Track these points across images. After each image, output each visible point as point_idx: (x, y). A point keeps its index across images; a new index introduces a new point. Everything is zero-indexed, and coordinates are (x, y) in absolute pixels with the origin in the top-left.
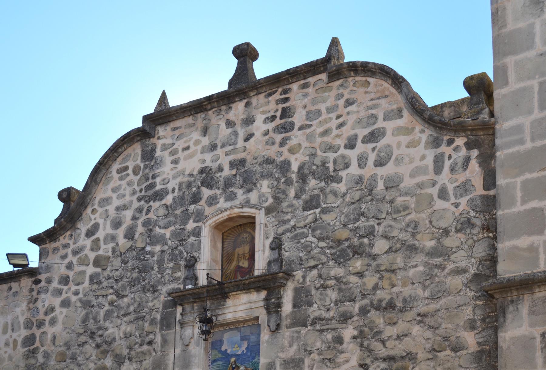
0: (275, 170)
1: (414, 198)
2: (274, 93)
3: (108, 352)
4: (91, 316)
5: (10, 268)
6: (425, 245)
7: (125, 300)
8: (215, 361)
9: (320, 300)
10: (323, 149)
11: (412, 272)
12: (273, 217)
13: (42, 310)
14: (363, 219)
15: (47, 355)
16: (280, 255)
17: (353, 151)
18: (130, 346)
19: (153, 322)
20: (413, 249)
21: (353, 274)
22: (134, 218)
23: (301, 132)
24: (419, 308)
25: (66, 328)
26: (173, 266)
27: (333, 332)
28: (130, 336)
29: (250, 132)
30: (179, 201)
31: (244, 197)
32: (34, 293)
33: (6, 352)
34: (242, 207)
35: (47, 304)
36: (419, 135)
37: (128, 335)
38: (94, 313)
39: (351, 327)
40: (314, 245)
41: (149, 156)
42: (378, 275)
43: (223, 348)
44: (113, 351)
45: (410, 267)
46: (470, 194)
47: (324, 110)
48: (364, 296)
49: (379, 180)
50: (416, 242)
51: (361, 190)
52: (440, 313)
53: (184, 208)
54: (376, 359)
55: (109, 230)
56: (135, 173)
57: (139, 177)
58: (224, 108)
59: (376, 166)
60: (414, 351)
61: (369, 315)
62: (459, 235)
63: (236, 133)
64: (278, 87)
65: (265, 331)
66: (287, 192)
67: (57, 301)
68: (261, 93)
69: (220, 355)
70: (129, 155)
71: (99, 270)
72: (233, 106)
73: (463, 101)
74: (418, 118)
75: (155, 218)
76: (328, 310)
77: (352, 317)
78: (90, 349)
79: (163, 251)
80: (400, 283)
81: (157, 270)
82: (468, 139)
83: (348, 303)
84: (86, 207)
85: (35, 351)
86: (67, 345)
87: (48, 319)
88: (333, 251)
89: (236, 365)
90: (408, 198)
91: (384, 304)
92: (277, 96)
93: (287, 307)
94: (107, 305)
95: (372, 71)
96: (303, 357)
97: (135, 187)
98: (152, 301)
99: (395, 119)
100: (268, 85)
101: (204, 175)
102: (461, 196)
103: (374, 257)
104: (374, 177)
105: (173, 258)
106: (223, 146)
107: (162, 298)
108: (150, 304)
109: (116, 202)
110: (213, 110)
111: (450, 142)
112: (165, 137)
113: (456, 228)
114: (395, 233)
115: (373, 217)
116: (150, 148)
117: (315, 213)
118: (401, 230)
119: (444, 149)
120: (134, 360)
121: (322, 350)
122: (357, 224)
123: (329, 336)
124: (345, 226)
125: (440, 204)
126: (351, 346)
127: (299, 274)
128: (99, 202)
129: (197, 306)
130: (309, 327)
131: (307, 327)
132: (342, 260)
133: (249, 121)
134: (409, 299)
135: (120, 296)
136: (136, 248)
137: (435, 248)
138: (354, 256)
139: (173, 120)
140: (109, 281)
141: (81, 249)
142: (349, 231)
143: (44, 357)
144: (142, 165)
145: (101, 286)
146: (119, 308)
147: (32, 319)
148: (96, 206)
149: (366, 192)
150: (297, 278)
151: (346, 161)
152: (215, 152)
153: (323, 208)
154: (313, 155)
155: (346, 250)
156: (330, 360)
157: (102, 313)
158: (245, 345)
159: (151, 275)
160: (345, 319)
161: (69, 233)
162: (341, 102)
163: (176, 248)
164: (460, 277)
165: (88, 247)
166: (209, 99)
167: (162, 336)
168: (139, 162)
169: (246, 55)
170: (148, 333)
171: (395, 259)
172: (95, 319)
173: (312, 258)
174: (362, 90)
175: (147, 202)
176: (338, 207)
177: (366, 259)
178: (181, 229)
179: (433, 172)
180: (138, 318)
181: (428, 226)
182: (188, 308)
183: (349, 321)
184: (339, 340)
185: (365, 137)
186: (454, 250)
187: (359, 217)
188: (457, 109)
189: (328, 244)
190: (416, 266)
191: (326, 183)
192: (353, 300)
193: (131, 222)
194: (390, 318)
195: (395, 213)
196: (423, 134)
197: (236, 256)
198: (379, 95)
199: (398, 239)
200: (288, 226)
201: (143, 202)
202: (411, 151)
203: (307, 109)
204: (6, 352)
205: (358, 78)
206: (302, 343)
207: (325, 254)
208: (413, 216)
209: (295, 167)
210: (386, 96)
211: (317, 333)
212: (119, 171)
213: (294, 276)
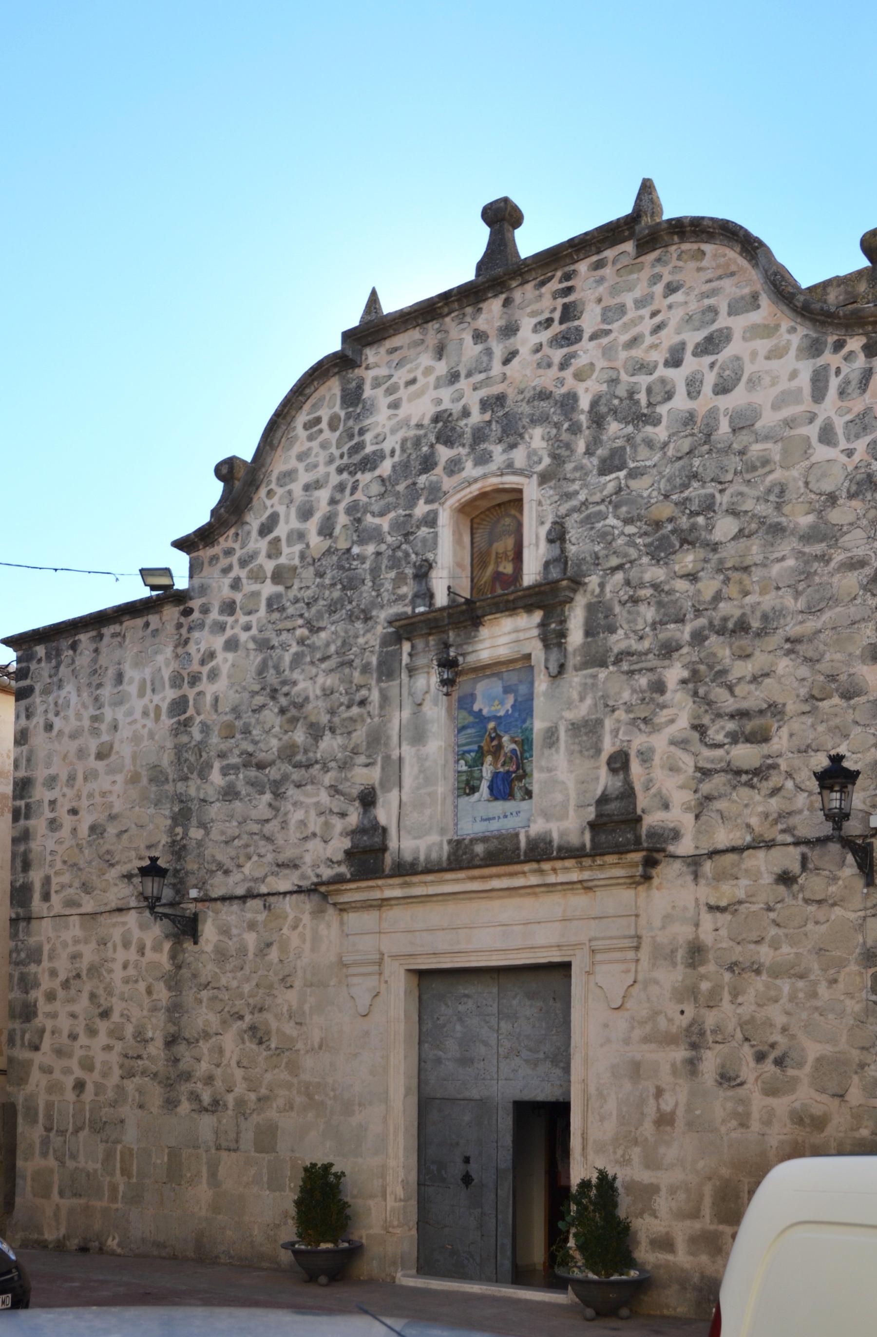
0: (552, 410)
1: (780, 444)
2: (550, 279)
3: (298, 720)
4: (270, 663)
5: (145, 592)
6: (797, 523)
7: (323, 635)
8: (464, 728)
9: (629, 622)
10: (631, 370)
11: (776, 569)
12: (551, 488)
13: (196, 658)
14: (695, 484)
15: (206, 729)
16: (563, 550)
17: (678, 369)
19: (366, 669)
20: (777, 530)
21: (681, 577)
22: (333, 502)
23: (593, 343)
24: (787, 628)
25: (233, 684)
27: (649, 674)
28: (332, 693)
29: (512, 349)
30: (403, 469)
31: (505, 457)
32: (184, 631)
33: (144, 726)
34: (502, 475)
35: (203, 647)
36: (787, 336)
37: (328, 692)
38: (275, 659)
39: (678, 665)
40: (616, 532)
41: (353, 398)
42: (722, 577)
43: (476, 708)
44: (305, 718)
45: (772, 561)
46: (871, 433)
47: (630, 304)
48: (698, 613)
49: (722, 418)
50: (783, 519)
51: (693, 435)
52: (822, 636)
53: (409, 481)
54: (719, 715)
55: (295, 524)
56: (333, 427)
57: (337, 433)
58: (469, 310)
59: (716, 393)
60: (780, 701)
61: (707, 643)
62: (855, 503)
63: (489, 352)
64: (556, 270)
65: (542, 677)
66: (573, 446)
67: (218, 643)
68: (528, 282)
69: (471, 719)
70: (322, 399)
71: (280, 589)
72: (484, 306)
73: (860, 274)
74: (785, 308)
75: (365, 499)
76: (641, 638)
77: (679, 648)
78: (270, 716)
79: (378, 554)
80: (757, 588)
81: (370, 584)
82: (869, 338)
83: (673, 626)
84: (258, 488)
85: (187, 723)
86: (236, 711)
87: (205, 670)
88: (648, 540)
90: (769, 445)
91: (730, 625)
92: (555, 285)
93: (576, 637)
94: (294, 644)
95: (708, 232)
97: (333, 450)
98: (364, 635)
99: (747, 311)
100: (539, 267)
101: (440, 425)
102: (857, 437)
103: (715, 547)
104: (713, 414)
105: (395, 563)
106: (469, 375)
107: (380, 630)
109: (304, 477)
110: (453, 315)
111: (839, 346)
112: (377, 365)
113: (848, 491)
114: (748, 505)
115: (712, 480)
116: (354, 384)
117: (618, 478)
118: (758, 499)
119: (830, 358)
120: (338, 731)
122: (686, 494)
123: (643, 681)
124: (666, 497)
125: (822, 452)
126: (679, 696)
127: (593, 581)
128: (278, 479)
130: (611, 668)
132: (662, 555)
133: (510, 330)
134: (771, 615)
135: (315, 630)
136: (337, 550)
137: (813, 527)
138: (681, 546)
139: (390, 337)
140: (297, 605)
141: (252, 556)
142: (672, 505)
143: (202, 732)
144: (342, 414)
145: (285, 615)
146: (313, 648)
147: (182, 672)
148: (273, 486)
149: (700, 439)
150: (590, 587)
151: (668, 388)
152: (457, 386)
154: (614, 382)
155: (668, 537)
156: (645, 720)
157: (287, 658)
158: (510, 700)
159: (361, 593)
161: (232, 531)
162: (659, 289)
163: (399, 547)
164: (856, 573)
165: (263, 553)
166: (446, 297)
167: (381, 691)
168: (337, 409)
169: (503, 219)
170: (359, 687)
171: (748, 548)
172: (276, 667)
173: (615, 553)
174: (692, 265)
175: (352, 474)
176: (654, 466)
177: (701, 550)
178: (406, 515)
179: (810, 399)
180: (342, 664)
181: (802, 490)
182: (420, 643)
183: (675, 655)
184: (659, 687)
185: (697, 345)
186: (845, 529)
187: (690, 480)
188: (850, 289)
189: (640, 528)
190: (783, 559)
191: (636, 426)
192: (681, 620)
193: (328, 509)
194: (741, 648)
195: (747, 471)
196: (793, 334)
197: (493, 556)
198: (720, 272)
199: (754, 516)
200: (575, 503)
201: (345, 475)
202: (774, 364)
203: (603, 304)
204: (144, 726)
205: (686, 246)
206: (600, 694)
207: (635, 545)
208: (777, 475)
209: (584, 403)
210: (732, 274)
211: (624, 677)
212: (307, 426)
213: (586, 584)
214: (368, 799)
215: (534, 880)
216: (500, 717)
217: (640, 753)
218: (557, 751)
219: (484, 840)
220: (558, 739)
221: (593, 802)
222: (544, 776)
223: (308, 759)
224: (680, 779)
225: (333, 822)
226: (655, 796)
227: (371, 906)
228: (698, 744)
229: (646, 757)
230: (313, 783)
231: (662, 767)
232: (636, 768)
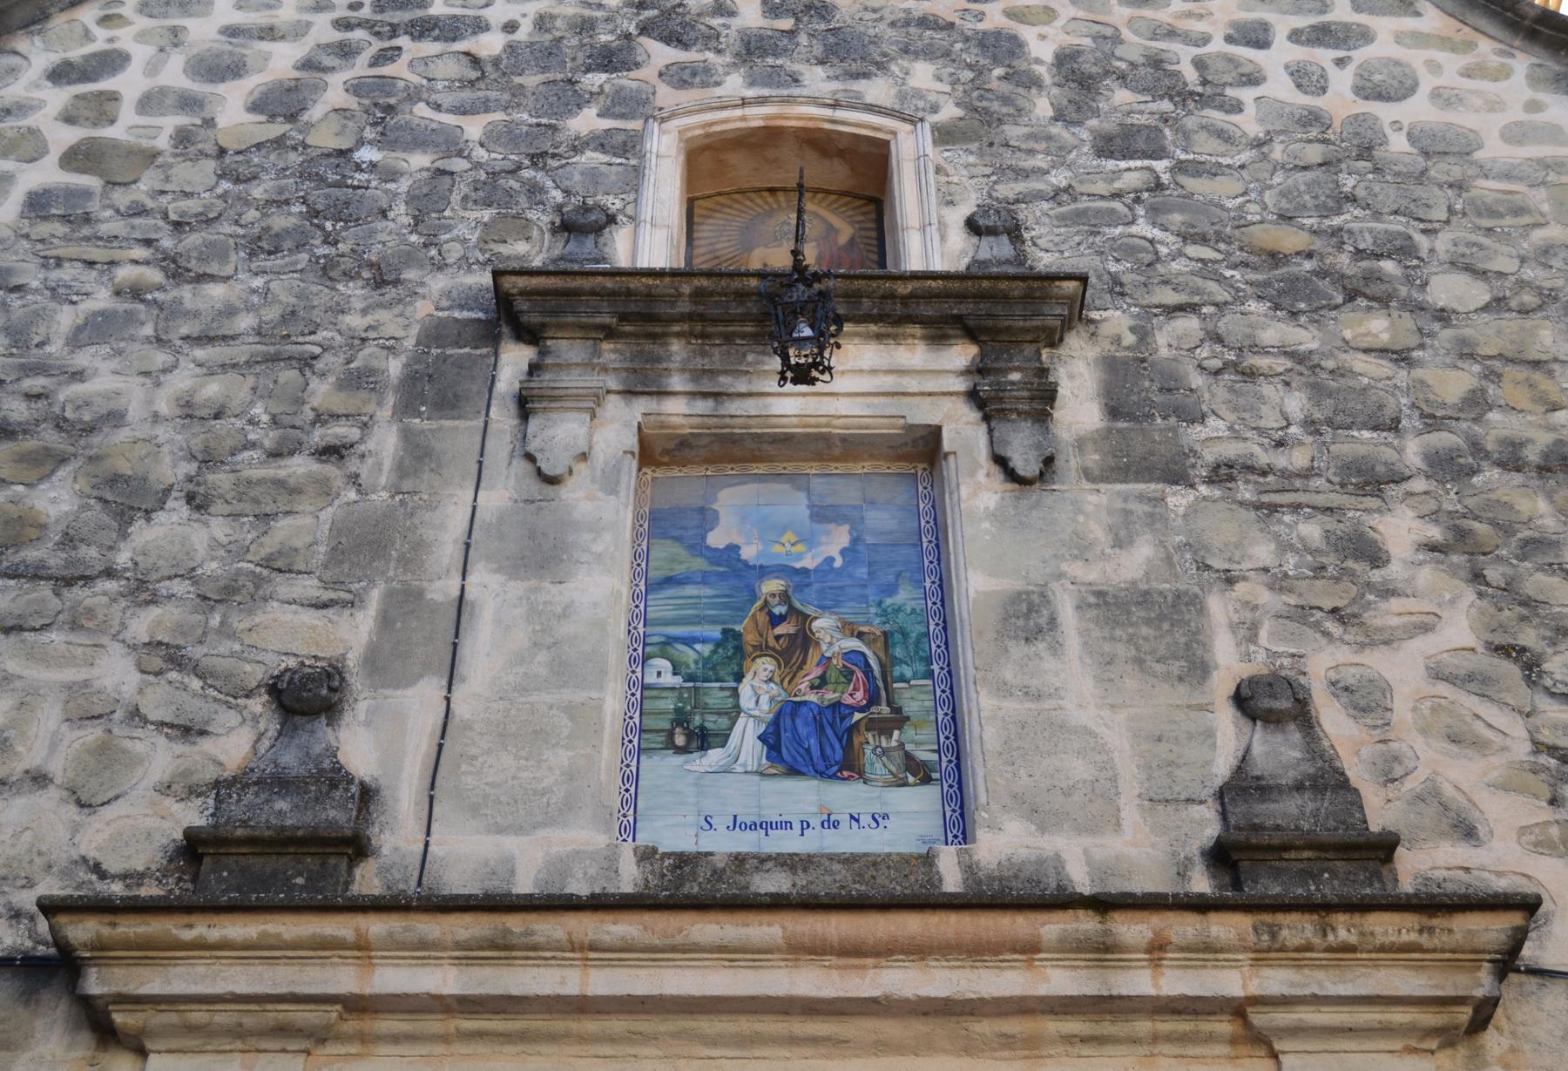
0: (958, 46)
7: (216, 291)
18: (206, 450)
21: (1367, 351)
26: (493, 220)
28: (217, 416)
40: (1163, 250)
48: (1432, 422)
51: (1325, 141)
65: (981, 476)
74: (1483, 23)
76: (1280, 444)
83: (1366, 434)
88: (1260, 277)
89: (792, 609)
96: (1196, 589)
98: (364, 312)
99: (1392, 13)
103: (1443, 316)
107: (423, 308)
108: (354, 321)
114: (1504, 262)
118: (1523, 260)
120: (219, 507)
121: (1286, 575)
122: (1336, 221)
126: (1426, 576)
127: (1116, 321)
129: (615, 351)
130: (1204, 490)
131: (1192, 486)
132: (1302, 305)
136: (306, 146)
140: (137, 221)
150: (1106, 330)
153: (1182, 162)
155: (1310, 280)
157: (66, 318)
160: (1367, 483)
163: (514, 171)
167: (407, 435)
173: (1166, 282)
176: (1242, 167)
180: (273, 359)
182: (568, 349)
183: (1392, 491)
192: (1394, 426)
195: (1479, 214)
206: (1181, 538)
207: (1220, 279)
214: (306, 698)
215: (1061, 980)
216: (805, 571)
217: (1341, 689)
218: (1056, 649)
219: (789, 862)
220: (1053, 621)
221: (1206, 793)
222: (1014, 707)
223: (69, 563)
224: (1495, 766)
225: (139, 747)
226: (1420, 798)
227: (282, 1030)
228: (1523, 689)
229: (1365, 700)
230: (75, 626)
231: (1424, 731)
232: (1334, 720)
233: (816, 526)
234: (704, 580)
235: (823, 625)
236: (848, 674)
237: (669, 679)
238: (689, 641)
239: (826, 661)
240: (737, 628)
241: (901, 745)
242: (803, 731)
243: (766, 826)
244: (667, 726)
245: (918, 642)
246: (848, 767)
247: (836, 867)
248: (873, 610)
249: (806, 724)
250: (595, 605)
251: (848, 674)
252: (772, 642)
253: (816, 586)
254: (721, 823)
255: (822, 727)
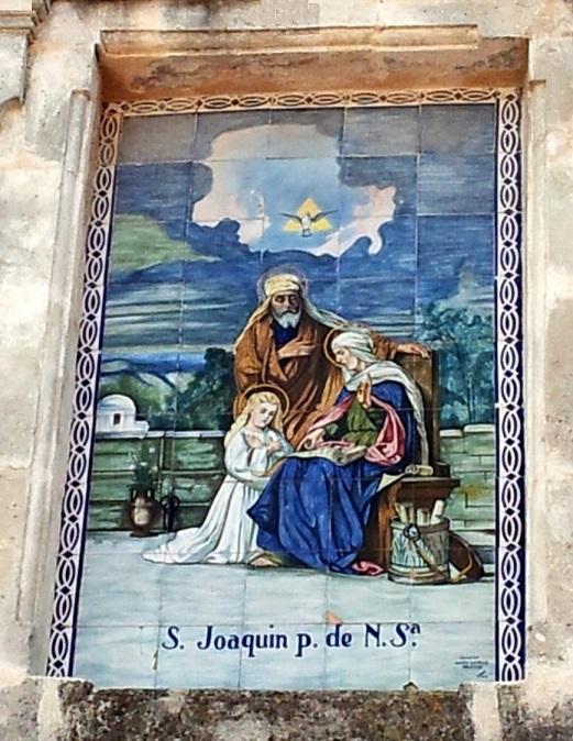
89: (306, 319)
216: (328, 260)
233: (348, 189)
234: (187, 274)
235: (349, 342)
236: (377, 417)
237: (131, 427)
238: (160, 369)
239: (348, 397)
240: (227, 348)
241: (445, 522)
242: (309, 501)
243: (250, 642)
244: (123, 495)
245: (480, 366)
246: (365, 554)
247: (331, 712)
248: (419, 319)
249: (315, 492)
250: (23, 328)
251: (377, 417)
252: (275, 370)
253: (342, 283)
254: (190, 636)
255: (337, 498)
